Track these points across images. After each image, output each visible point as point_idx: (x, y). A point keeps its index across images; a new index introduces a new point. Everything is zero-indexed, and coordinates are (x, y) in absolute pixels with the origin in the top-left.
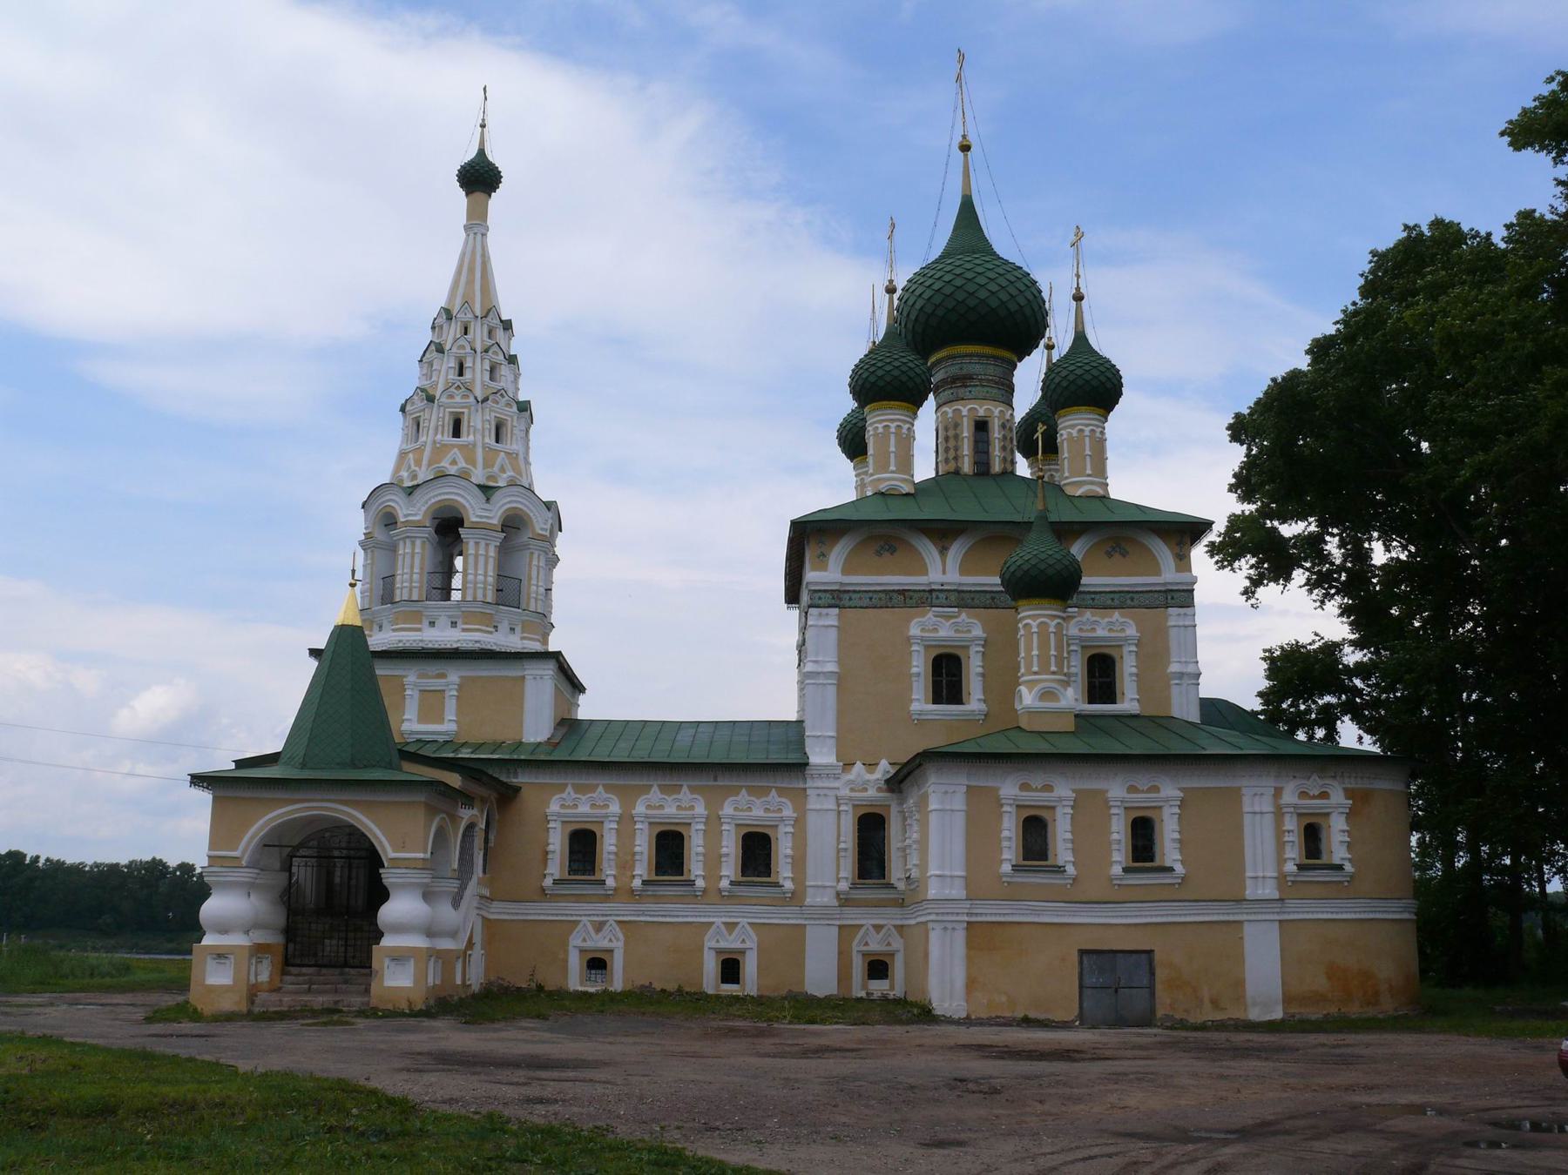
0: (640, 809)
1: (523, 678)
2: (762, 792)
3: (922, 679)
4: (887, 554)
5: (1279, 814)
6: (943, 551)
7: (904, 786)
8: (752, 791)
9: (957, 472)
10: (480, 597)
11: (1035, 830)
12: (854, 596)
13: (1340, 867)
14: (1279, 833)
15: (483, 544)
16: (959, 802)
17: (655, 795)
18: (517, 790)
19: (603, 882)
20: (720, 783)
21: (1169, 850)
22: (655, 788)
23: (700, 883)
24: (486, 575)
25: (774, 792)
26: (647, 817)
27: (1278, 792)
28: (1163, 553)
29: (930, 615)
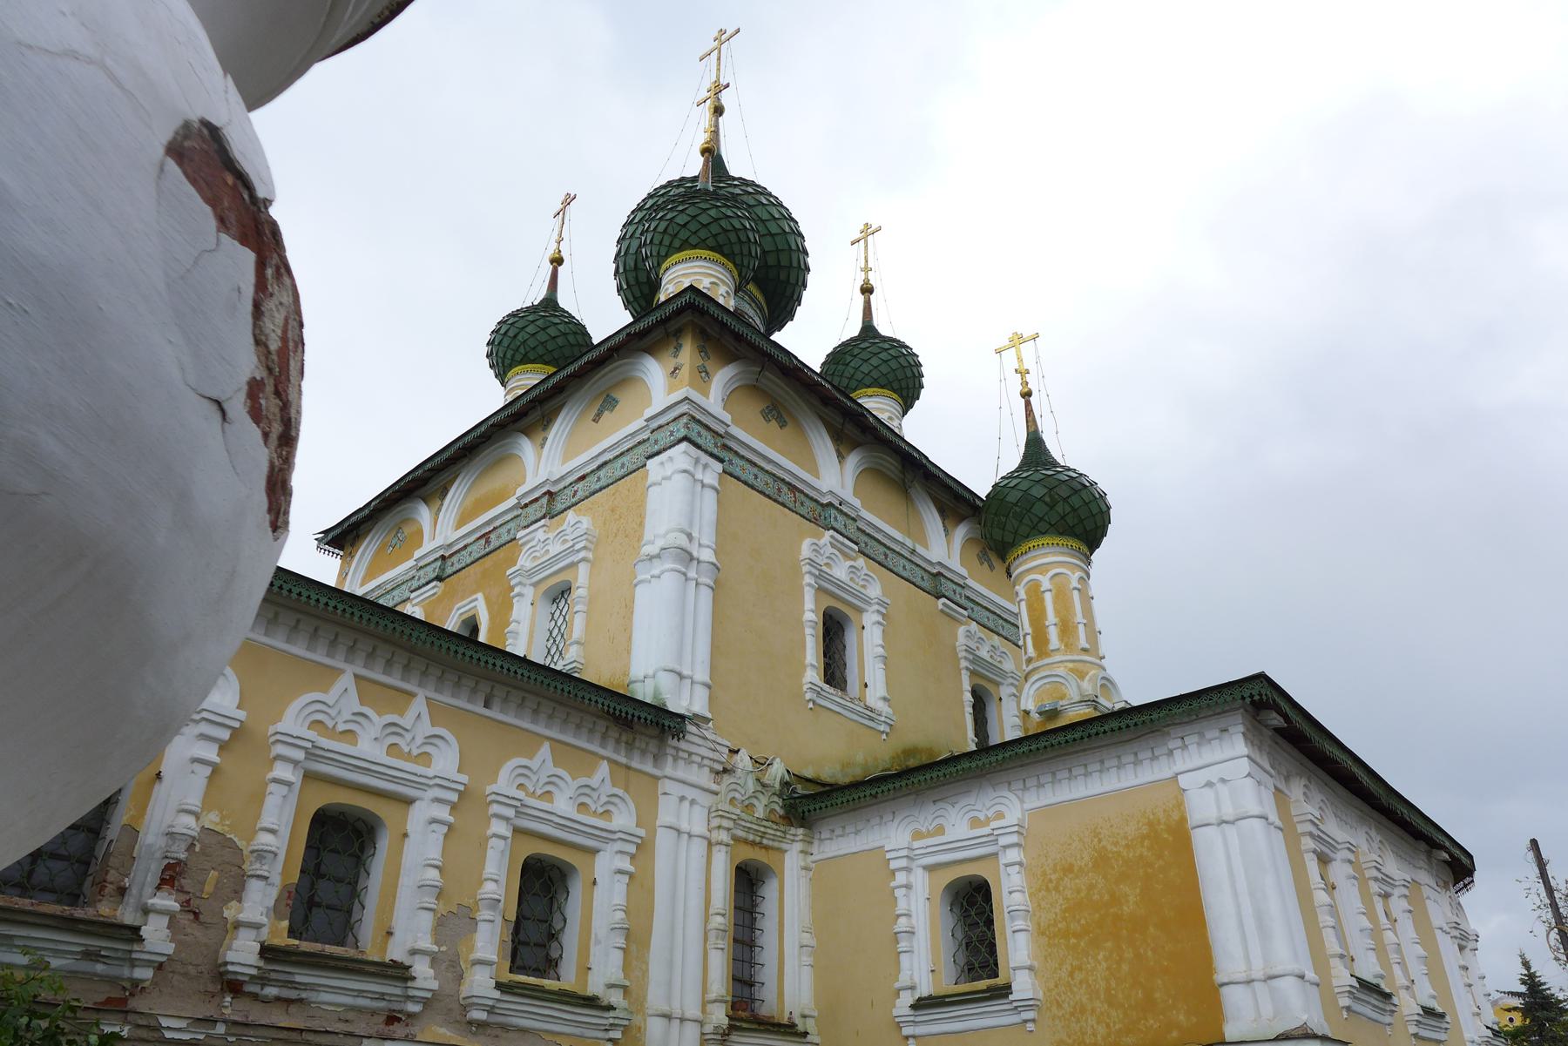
17: (342, 694)
19: (133, 934)
20: (493, 713)
22: (346, 681)
26: (313, 753)
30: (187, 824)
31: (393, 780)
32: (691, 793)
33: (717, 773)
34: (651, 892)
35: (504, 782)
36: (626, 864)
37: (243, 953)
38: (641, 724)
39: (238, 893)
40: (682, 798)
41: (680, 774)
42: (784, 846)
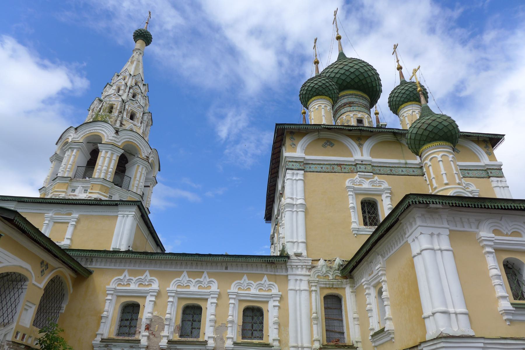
1: (117, 216)
2: (257, 277)
6: (360, 145)
7: (356, 273)
8: (251, 276)
10: (102, 176)
12: (312, 166)
15: (110, 152)
17: (184, 278)
18: (90, 273)
20: (229, 271)
22: (185, 274)
25: (265, 278)
26: (177, 293)
29: (357, 176)
31: (200, 295)
32: (299, 278)
33: (310, 269)
34: (287, 310)
36: (277, 303)
38: (279, 262)
39: (163, 329)
40: (296, 280)
41: (294, 273)
42: (343, 286)
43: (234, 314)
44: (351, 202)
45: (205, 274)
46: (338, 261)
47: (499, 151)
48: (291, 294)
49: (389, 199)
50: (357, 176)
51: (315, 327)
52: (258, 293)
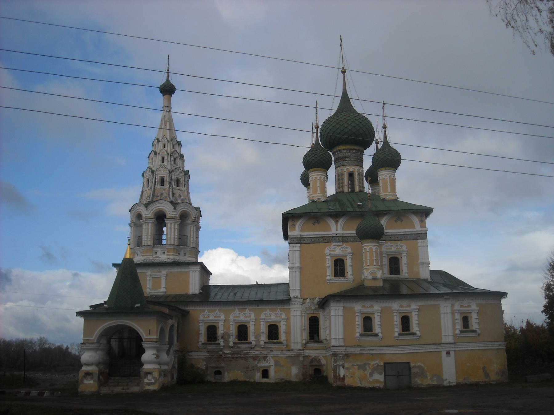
0: (231, 317)
1: (189, 271)
3: (330, 268)
4: (316, 224)
5: (453, 313)
6: (337, 222)
9: (343, 192)
10: (172, 243)
11: (368, 321)
13: (475, 331)
14: (454, 320)
15: (173, 224)
16: (340, 312)
17: (237, 312)
21: (415, 327)
22: (237, 310)
23: (254, 343)
24: (174, 235)
27: (453, 306)
28: (415, 220)
30: (222, 332)
32: (296, 309)
35: (263, 317)
36: (285, 323)
37: (231, 344)
39: (230, 338)
43: (264, 329)
44: (327, 262)
45: (247, 310)
46: (317, 299)
47: (429, 221)
48: (292, 318)
49: (350, 259)
50: (333, 244)
51: (304, 334)
52: (275, 318)
